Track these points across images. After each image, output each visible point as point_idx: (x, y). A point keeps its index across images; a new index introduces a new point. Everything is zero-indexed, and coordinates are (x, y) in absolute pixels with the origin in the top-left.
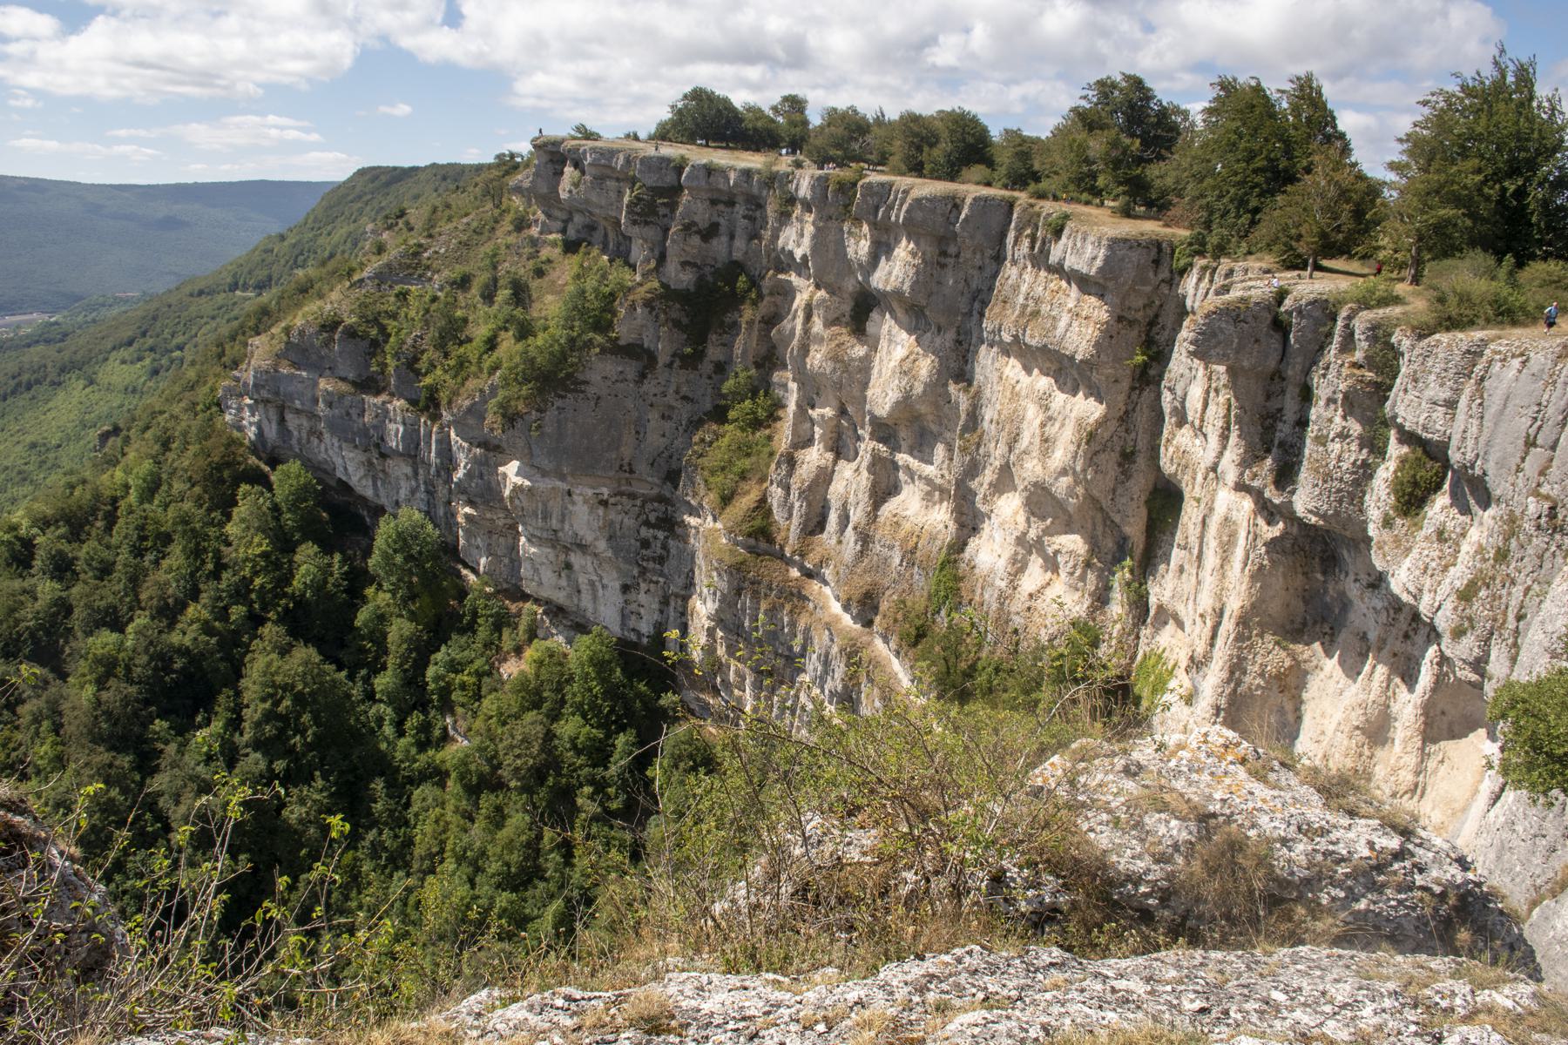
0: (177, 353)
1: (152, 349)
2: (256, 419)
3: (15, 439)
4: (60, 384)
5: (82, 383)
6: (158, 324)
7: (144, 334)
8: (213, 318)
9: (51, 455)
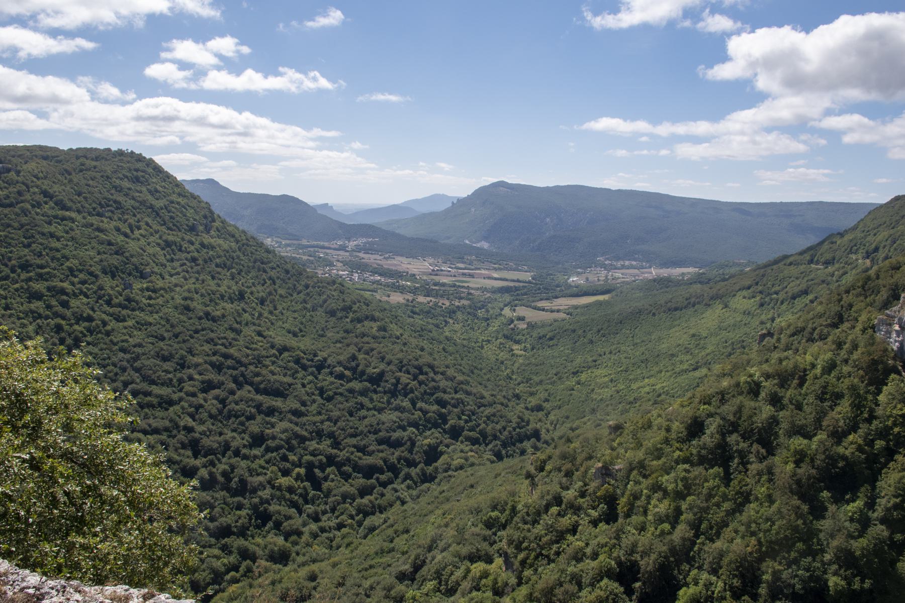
0: (775, 296)
1: (761, 292)
2: (900, 339)
3: (685, 331)
4: (709, 305)
5: (721, 306)
6: (765, 279)
7: (757, 284)
8: (797, 278)
9: (702, 342)
